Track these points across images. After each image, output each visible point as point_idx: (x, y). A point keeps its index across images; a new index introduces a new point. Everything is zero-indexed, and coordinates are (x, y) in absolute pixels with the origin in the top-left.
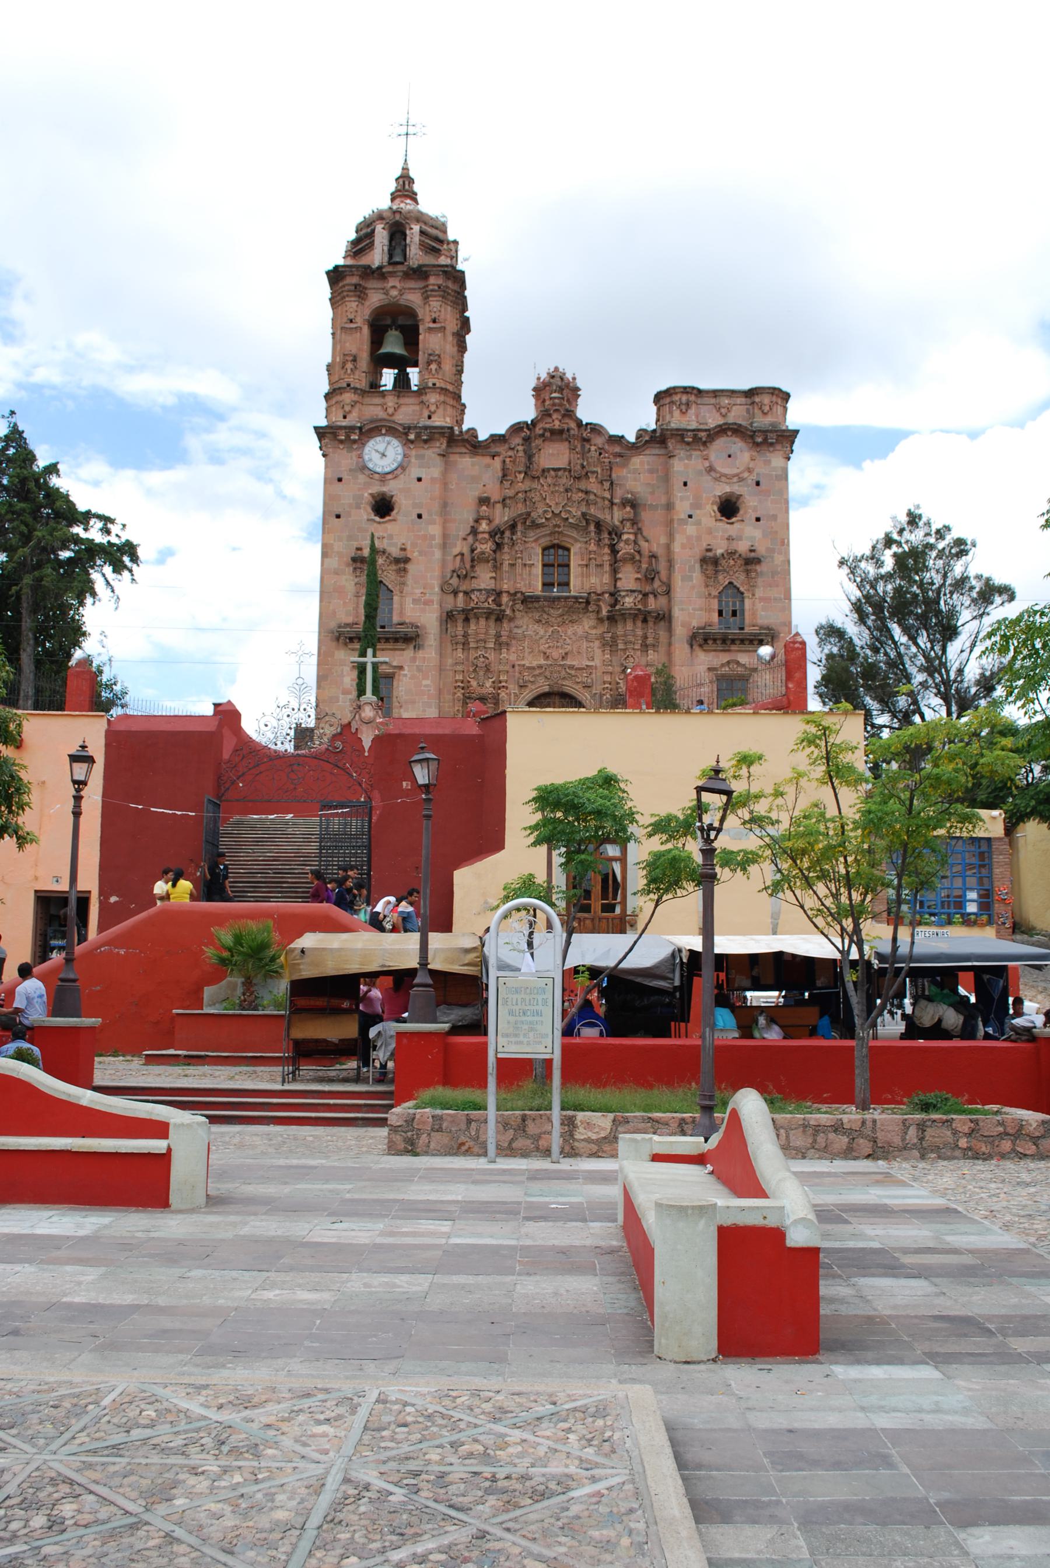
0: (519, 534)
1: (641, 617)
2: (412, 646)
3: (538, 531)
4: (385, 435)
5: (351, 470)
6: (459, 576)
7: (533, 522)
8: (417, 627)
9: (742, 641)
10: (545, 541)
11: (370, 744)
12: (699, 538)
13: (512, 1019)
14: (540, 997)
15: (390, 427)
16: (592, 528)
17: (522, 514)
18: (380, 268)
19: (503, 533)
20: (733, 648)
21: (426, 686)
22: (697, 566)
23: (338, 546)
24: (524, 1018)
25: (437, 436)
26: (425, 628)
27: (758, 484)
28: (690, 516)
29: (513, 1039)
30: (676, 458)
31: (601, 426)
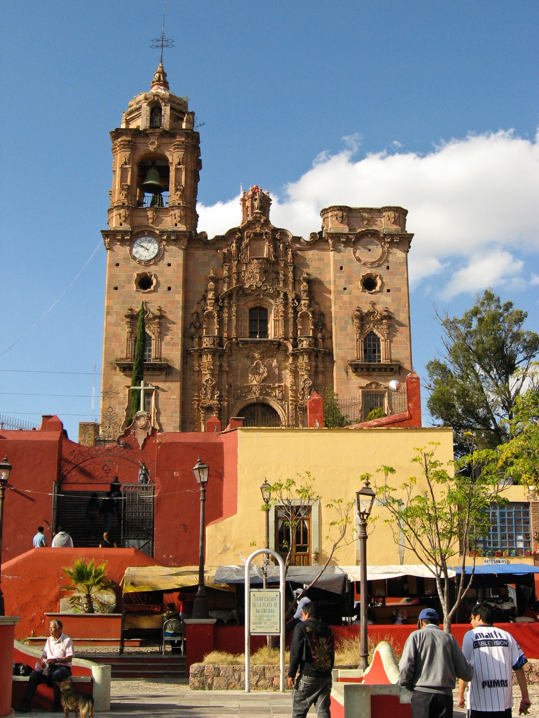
0: (234, 299)
1: (314, 354)
2: (164, 373)
3: (246, 298)
4: (147, 236)
5: (125, 259)
6: (195, 327)
8: (168, 361)
9: (380, 370)
10: (251, 305)
11: (143, 442)
12: (351, 303)
13: (258, 614)
14: (273, 602)
15: (150, 231)
18: (145, 130)
20: (374, 373)
21: (173, 399)
22: (350, 320)
23: (117, 308)
24: (265, 614)
25: (181, 237)
26: (173, 361)
27: (388, 268)
28: (345, 289)
29: (259, 625)
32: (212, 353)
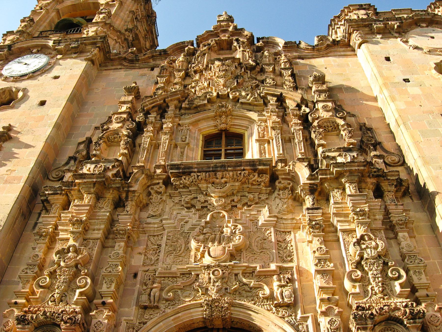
1: (371, 181)
19: (147, 114)
25: (89, 47)
32: (92, 190)
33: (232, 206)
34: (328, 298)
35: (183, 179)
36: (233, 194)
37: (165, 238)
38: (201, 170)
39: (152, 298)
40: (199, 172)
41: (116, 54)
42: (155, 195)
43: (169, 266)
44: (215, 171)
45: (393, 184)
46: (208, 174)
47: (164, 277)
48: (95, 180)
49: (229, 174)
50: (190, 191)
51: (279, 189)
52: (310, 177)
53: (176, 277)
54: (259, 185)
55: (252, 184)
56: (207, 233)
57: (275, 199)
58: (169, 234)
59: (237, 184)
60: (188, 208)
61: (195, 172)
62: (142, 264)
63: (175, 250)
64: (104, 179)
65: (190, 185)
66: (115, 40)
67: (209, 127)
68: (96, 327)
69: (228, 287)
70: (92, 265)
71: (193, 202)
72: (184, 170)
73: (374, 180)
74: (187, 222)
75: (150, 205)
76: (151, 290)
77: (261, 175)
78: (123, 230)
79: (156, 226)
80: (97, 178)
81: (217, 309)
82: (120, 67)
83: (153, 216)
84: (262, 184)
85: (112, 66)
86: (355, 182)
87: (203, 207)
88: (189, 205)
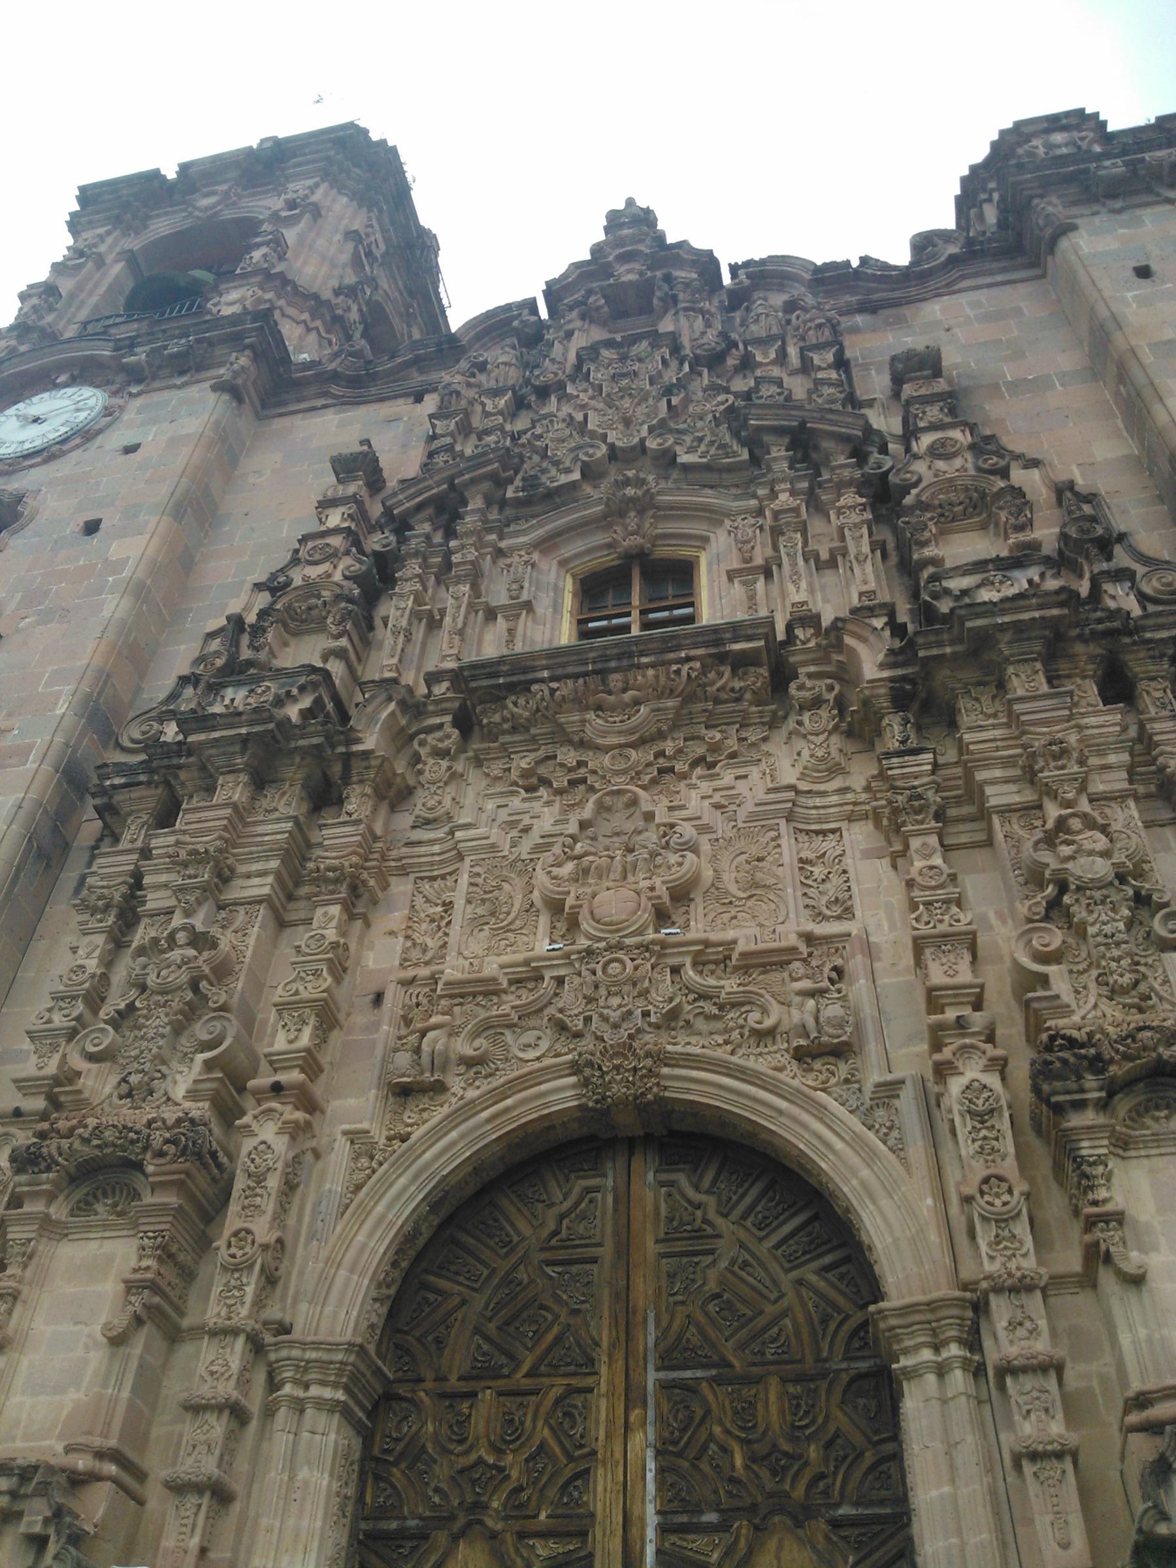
7: (531, 483)
16: (778, 453)
17: (479, 460)
19: (401, 526)
30: (1083, 232)
31: (784, 259)
33: (661, 771)
34: (959, 1017)
35: (511, 705)
36: (661, 736)
37: (464, 879)
38: (560, 672)
39: (425, 1059)
40: (553, 679)
41: (306, 366)
42: (431, 761)
43: (476, 962)
44: (602, 673)
45: (1162, 656)
46: (581, 681)
47: (462, 996)
48: (243, 731)
49: (644, 676)
50: (533, 739)
51: (801, 708)
52: (892, 659)
53: (496, 993)
54: (737, 700)
55: (717, 701)
56: (586, 854)
57: (789, 738)
58: (477, 869)
59: (670, 703)
60: (529, 789)
61: (542, 681)
62: (397, 963)
63: (493, 914)
64: (271, 726)
65: (531, 722)
66: (304, 322)
67: (588, 551)
68: (253, 1161)
69: (650, 1007)
70: (242, 978)
71: (542, 771)
72: (509, 679)
73: (1095, 649)
74: (526, 830)
75: (420, 792)
76: (423, 1035)
77: (740, 672)
78: (333, 869)
79: (436, 848)
80: (251, 723)
81: (618, 1078)
82: (323, 402)
83: (428, 822)
84: (748, 696)
85: (300, 400)
86: (1035, 660)
87: (573, 783)
88: (534, 780)
